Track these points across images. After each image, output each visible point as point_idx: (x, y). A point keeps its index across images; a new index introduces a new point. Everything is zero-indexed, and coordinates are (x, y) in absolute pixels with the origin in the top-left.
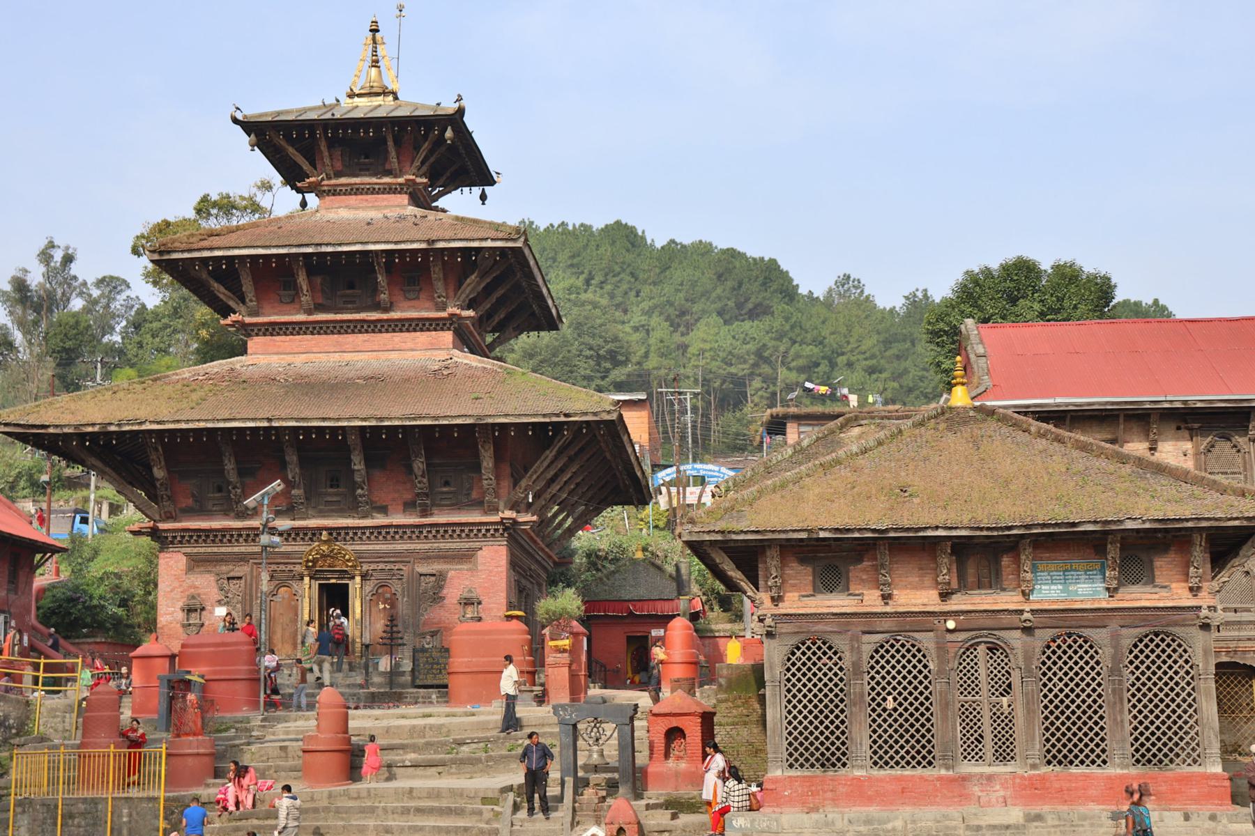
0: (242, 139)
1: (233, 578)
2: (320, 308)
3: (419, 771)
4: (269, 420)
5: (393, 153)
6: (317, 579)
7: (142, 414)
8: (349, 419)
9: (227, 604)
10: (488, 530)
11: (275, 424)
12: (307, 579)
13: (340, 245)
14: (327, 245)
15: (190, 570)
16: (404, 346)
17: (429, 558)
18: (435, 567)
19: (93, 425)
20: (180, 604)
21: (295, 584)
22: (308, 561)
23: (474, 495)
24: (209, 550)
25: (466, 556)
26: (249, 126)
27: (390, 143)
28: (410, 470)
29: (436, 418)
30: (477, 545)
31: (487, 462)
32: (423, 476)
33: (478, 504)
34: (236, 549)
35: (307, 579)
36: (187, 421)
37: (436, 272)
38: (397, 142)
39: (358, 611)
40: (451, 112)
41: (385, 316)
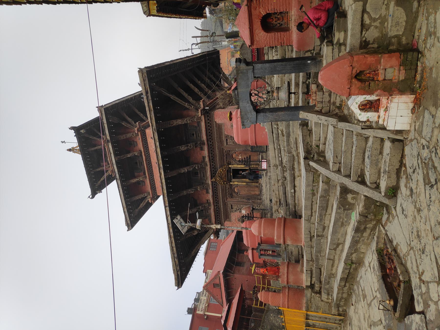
0: (98, 196)
1: (232, 207)
3: (297, 183)
5: (96, 148)
6: (231, 180)
9: (241, 209)
10: (208, 120)
12: (231, 183)
15: (230, 221)
17: (220, 141)
22: (224, 184)
23: (196, 125)
26: (94, 193)
27: (93, 149)
28: (187, 150)
30: (214, 123)
31: (179, 122)
32: (188, 146)
33: (199, 123)
35: (231, 183)
37: (123, 137)
38: (95, 146)
39: (242, 166)
40: (73, 131)
41: (143, 153)
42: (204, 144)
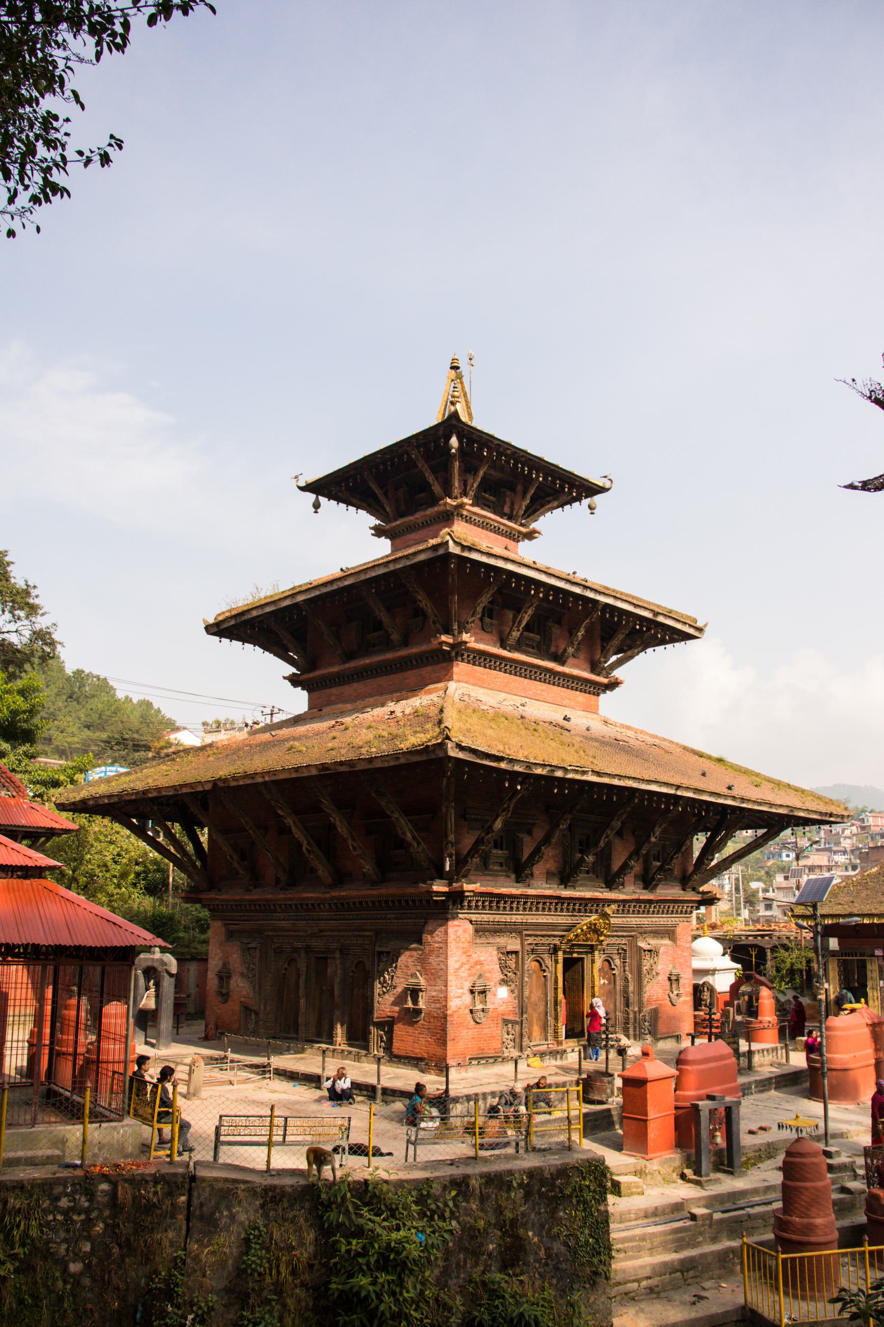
2: (518, 647)
4: (678, 787)
7: (585, 762)
8: (726, 797)
11: (679, 793)
13: (600, 593)
14: (592, 589)
15: (473, 943)
16: (566, 702)
18: (654, 942)
19: (544, 766)
20: (467, 985)
21: (548, 961)
24: (491, 918)
25: (669, 933)
29: (771, 805)
34: (514, 918)
35: (560, 953)
36: (620, 777)
42: (655, 888)
